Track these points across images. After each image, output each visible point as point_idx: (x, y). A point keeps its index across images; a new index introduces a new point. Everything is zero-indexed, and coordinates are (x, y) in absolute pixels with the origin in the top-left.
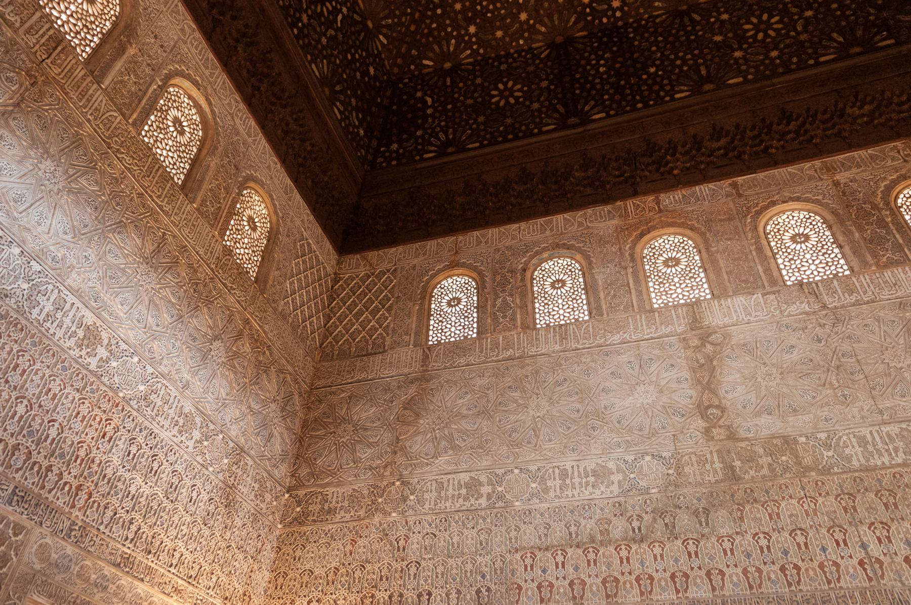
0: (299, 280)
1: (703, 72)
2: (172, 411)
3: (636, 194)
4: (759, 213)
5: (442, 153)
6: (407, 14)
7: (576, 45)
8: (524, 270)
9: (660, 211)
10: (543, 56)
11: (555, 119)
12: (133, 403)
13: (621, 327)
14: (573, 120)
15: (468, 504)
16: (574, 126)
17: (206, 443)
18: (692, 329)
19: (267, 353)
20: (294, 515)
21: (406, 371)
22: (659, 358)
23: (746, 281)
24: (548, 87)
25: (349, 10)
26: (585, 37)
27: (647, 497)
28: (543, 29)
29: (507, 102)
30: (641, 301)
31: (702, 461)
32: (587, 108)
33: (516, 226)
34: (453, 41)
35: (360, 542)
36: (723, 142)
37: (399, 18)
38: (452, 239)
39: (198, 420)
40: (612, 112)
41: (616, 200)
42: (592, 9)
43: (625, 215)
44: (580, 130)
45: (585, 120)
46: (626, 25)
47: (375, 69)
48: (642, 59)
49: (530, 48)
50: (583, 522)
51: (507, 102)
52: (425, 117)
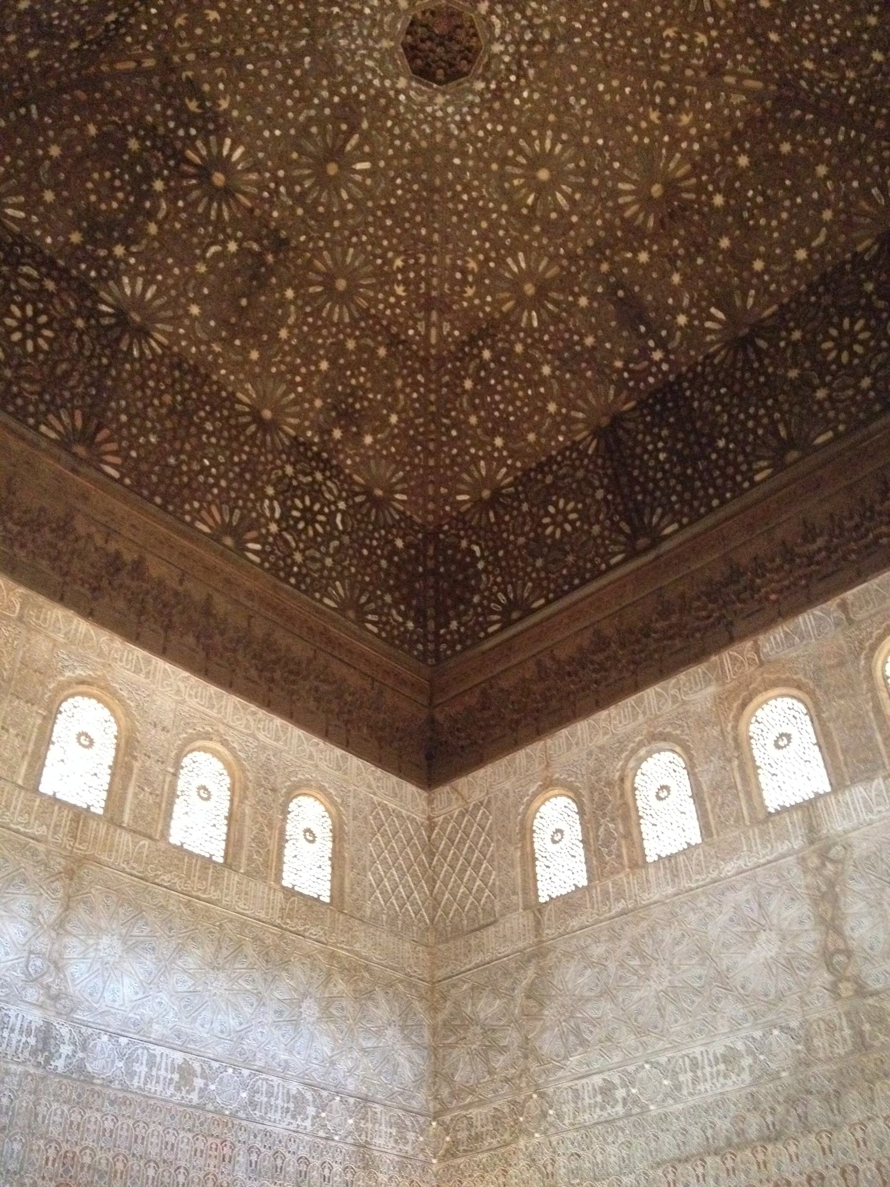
0: (384, 862)
1: (783, 433)
2: (279, 1102)
3: (731, 640)
4: (873, 648)
5: (507, 623)
6: (417, 454)
7: (625, 425)
8: (622, 780)
9: (762, 664)
10: (590, 452)
11: (621, 544)
12: (241, 1114)
13: (733, 851)
14: (642, 542)
15: (605, 1114)
16: (646, 550)
17: (323, 1115)
18: (812, 842)
19: (367, 975)
20: (445, 1146)
21: (521, 945)
22: (776, 888)
23: (865, 761)
24: (605, 499)
25: (346, 500)
26: (633, 409)
27: (778, 1083)
28: (580, 415)
29: (564, 531)
30: (751, 808)
31: (831, 1028)
32: (655, 520)
33: (604, 714)
34: (482, 463)
35: (512, 1171)
36: (820, 542)
37: (411, 463)
38: (539, 745)
39: (309, 1096)
40: (685, 520)
41: (710, 654)
42: (630, 371)
43: (721, 679)
44: (651, 556)
45: (657, 540)
46: (680, 377)
47: (403, 538)
48: (707, 430)
49: (574, 443)
50: (719, 1123)
51: (564, 531)
52: (477, 574)
